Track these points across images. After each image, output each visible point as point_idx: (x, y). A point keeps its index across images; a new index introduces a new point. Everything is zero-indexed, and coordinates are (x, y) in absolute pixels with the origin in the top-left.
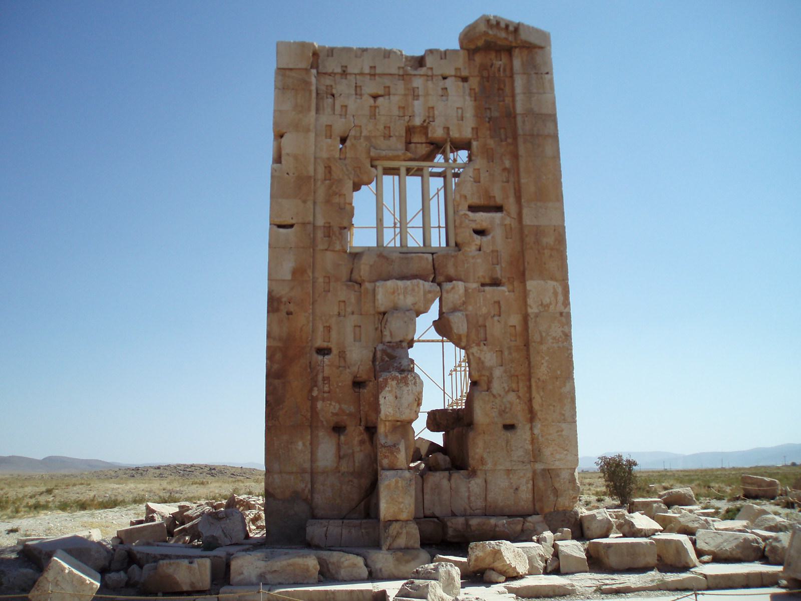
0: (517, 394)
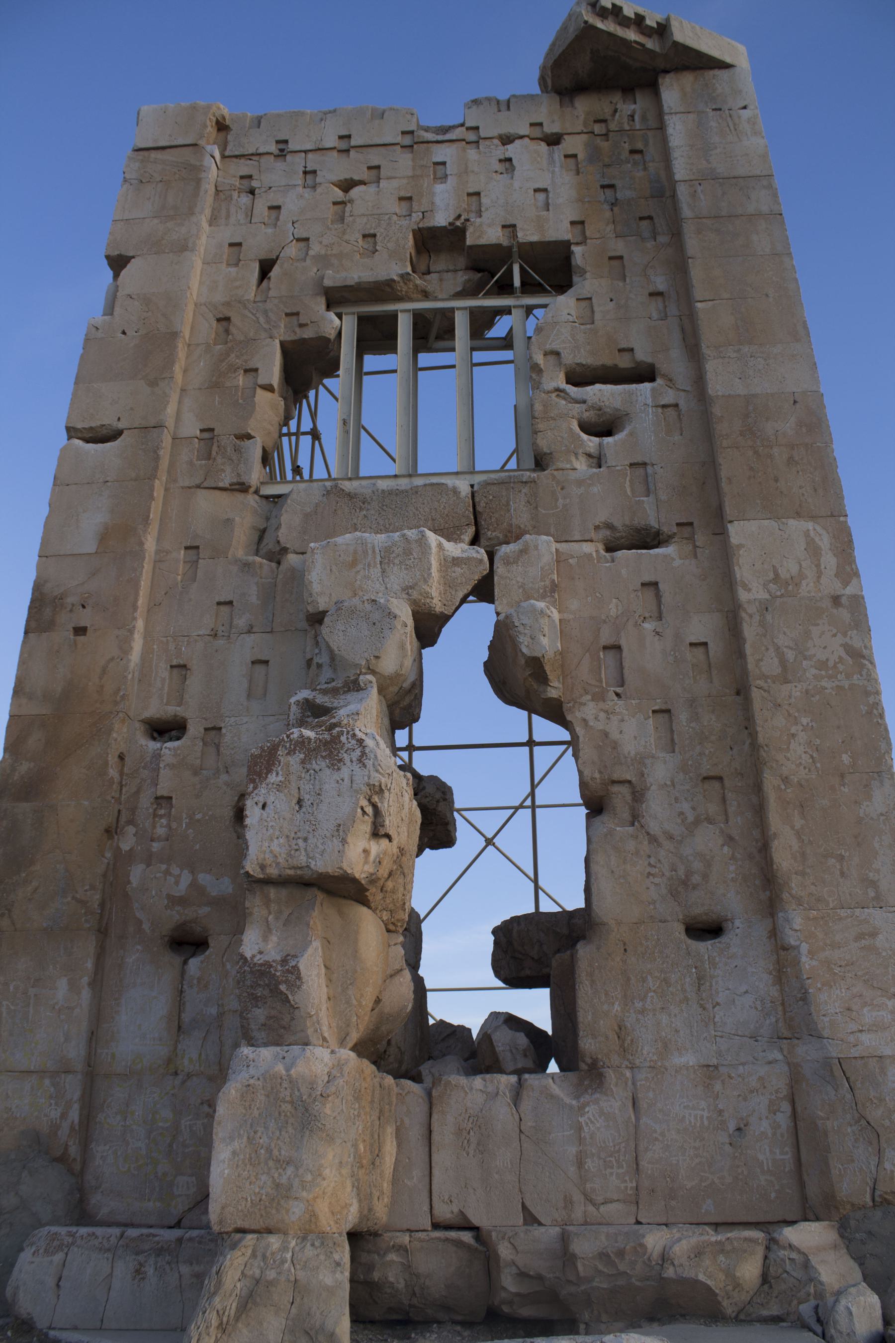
0: (722, 831)
